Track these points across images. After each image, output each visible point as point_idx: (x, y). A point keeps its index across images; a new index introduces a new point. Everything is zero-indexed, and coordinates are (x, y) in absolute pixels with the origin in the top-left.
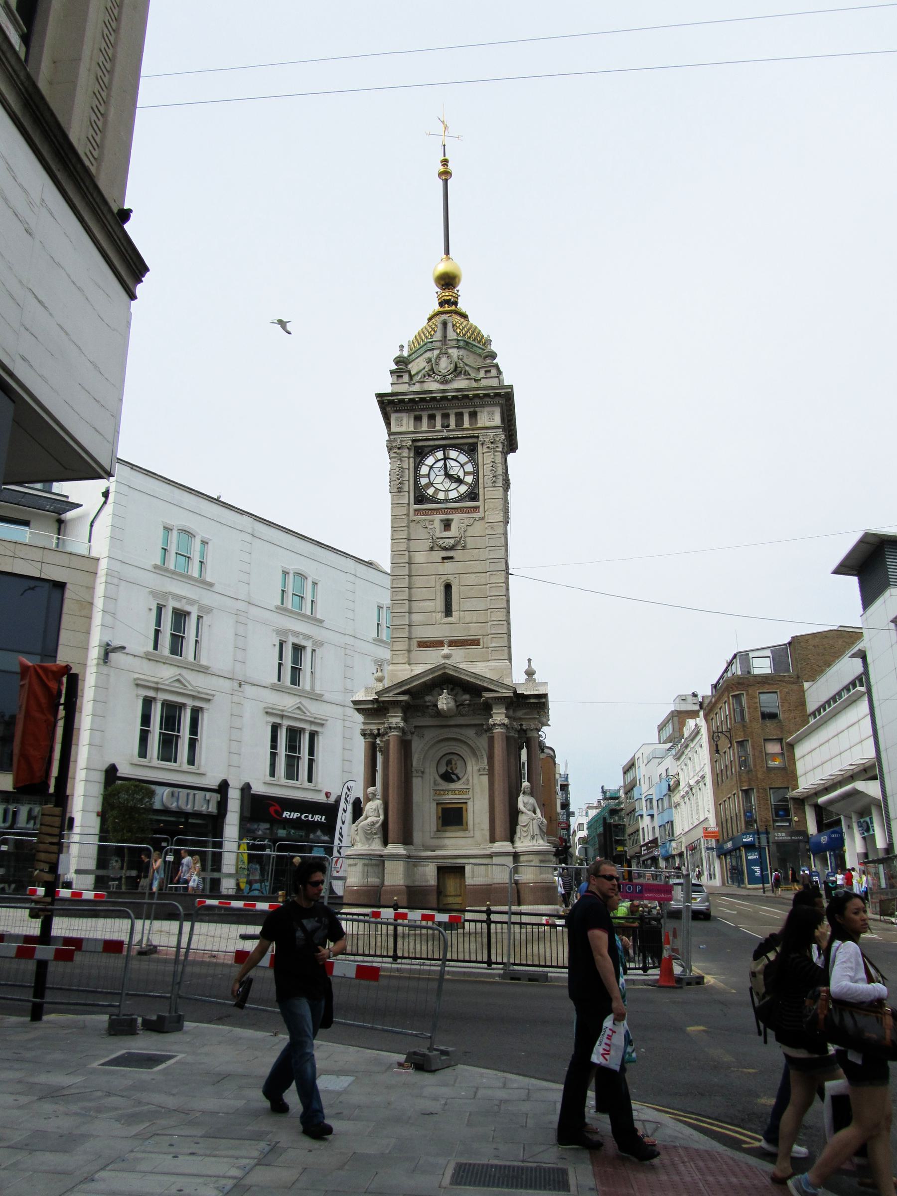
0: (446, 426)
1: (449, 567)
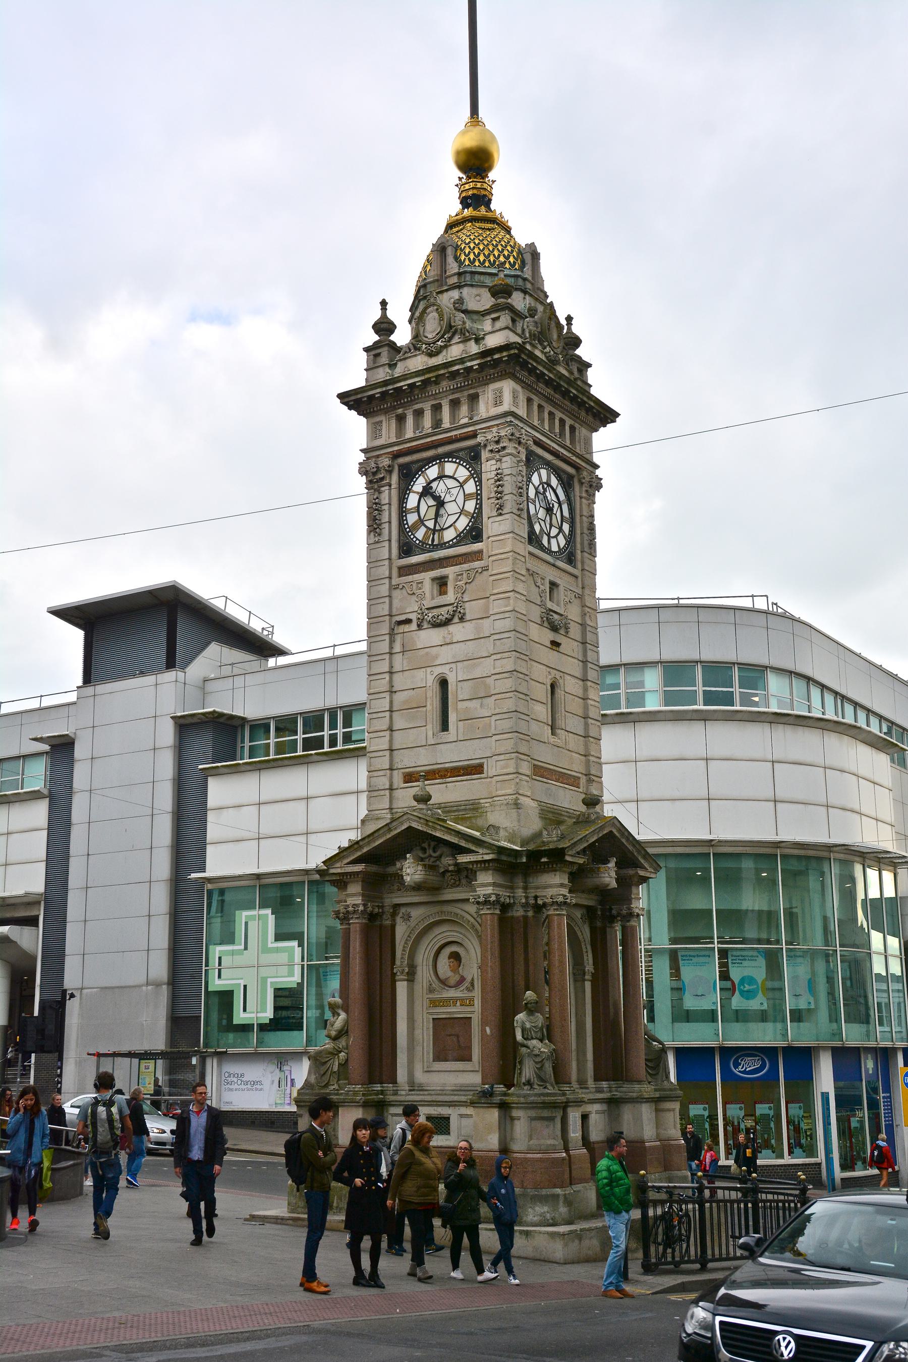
0: (437, 423)
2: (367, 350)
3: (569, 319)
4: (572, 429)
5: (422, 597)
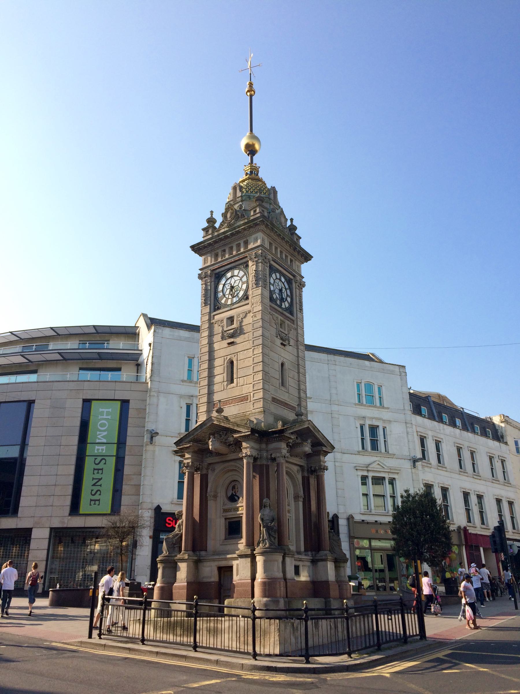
1: (232, 349)
2: (203, 230)
3: (292, 220)
4: (291, 261)
5: (223, 327)
